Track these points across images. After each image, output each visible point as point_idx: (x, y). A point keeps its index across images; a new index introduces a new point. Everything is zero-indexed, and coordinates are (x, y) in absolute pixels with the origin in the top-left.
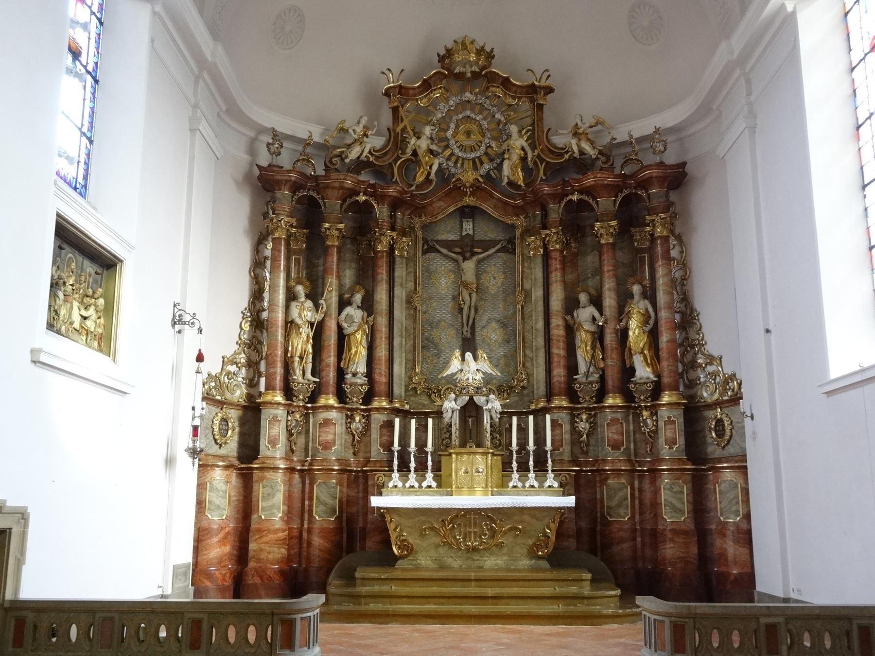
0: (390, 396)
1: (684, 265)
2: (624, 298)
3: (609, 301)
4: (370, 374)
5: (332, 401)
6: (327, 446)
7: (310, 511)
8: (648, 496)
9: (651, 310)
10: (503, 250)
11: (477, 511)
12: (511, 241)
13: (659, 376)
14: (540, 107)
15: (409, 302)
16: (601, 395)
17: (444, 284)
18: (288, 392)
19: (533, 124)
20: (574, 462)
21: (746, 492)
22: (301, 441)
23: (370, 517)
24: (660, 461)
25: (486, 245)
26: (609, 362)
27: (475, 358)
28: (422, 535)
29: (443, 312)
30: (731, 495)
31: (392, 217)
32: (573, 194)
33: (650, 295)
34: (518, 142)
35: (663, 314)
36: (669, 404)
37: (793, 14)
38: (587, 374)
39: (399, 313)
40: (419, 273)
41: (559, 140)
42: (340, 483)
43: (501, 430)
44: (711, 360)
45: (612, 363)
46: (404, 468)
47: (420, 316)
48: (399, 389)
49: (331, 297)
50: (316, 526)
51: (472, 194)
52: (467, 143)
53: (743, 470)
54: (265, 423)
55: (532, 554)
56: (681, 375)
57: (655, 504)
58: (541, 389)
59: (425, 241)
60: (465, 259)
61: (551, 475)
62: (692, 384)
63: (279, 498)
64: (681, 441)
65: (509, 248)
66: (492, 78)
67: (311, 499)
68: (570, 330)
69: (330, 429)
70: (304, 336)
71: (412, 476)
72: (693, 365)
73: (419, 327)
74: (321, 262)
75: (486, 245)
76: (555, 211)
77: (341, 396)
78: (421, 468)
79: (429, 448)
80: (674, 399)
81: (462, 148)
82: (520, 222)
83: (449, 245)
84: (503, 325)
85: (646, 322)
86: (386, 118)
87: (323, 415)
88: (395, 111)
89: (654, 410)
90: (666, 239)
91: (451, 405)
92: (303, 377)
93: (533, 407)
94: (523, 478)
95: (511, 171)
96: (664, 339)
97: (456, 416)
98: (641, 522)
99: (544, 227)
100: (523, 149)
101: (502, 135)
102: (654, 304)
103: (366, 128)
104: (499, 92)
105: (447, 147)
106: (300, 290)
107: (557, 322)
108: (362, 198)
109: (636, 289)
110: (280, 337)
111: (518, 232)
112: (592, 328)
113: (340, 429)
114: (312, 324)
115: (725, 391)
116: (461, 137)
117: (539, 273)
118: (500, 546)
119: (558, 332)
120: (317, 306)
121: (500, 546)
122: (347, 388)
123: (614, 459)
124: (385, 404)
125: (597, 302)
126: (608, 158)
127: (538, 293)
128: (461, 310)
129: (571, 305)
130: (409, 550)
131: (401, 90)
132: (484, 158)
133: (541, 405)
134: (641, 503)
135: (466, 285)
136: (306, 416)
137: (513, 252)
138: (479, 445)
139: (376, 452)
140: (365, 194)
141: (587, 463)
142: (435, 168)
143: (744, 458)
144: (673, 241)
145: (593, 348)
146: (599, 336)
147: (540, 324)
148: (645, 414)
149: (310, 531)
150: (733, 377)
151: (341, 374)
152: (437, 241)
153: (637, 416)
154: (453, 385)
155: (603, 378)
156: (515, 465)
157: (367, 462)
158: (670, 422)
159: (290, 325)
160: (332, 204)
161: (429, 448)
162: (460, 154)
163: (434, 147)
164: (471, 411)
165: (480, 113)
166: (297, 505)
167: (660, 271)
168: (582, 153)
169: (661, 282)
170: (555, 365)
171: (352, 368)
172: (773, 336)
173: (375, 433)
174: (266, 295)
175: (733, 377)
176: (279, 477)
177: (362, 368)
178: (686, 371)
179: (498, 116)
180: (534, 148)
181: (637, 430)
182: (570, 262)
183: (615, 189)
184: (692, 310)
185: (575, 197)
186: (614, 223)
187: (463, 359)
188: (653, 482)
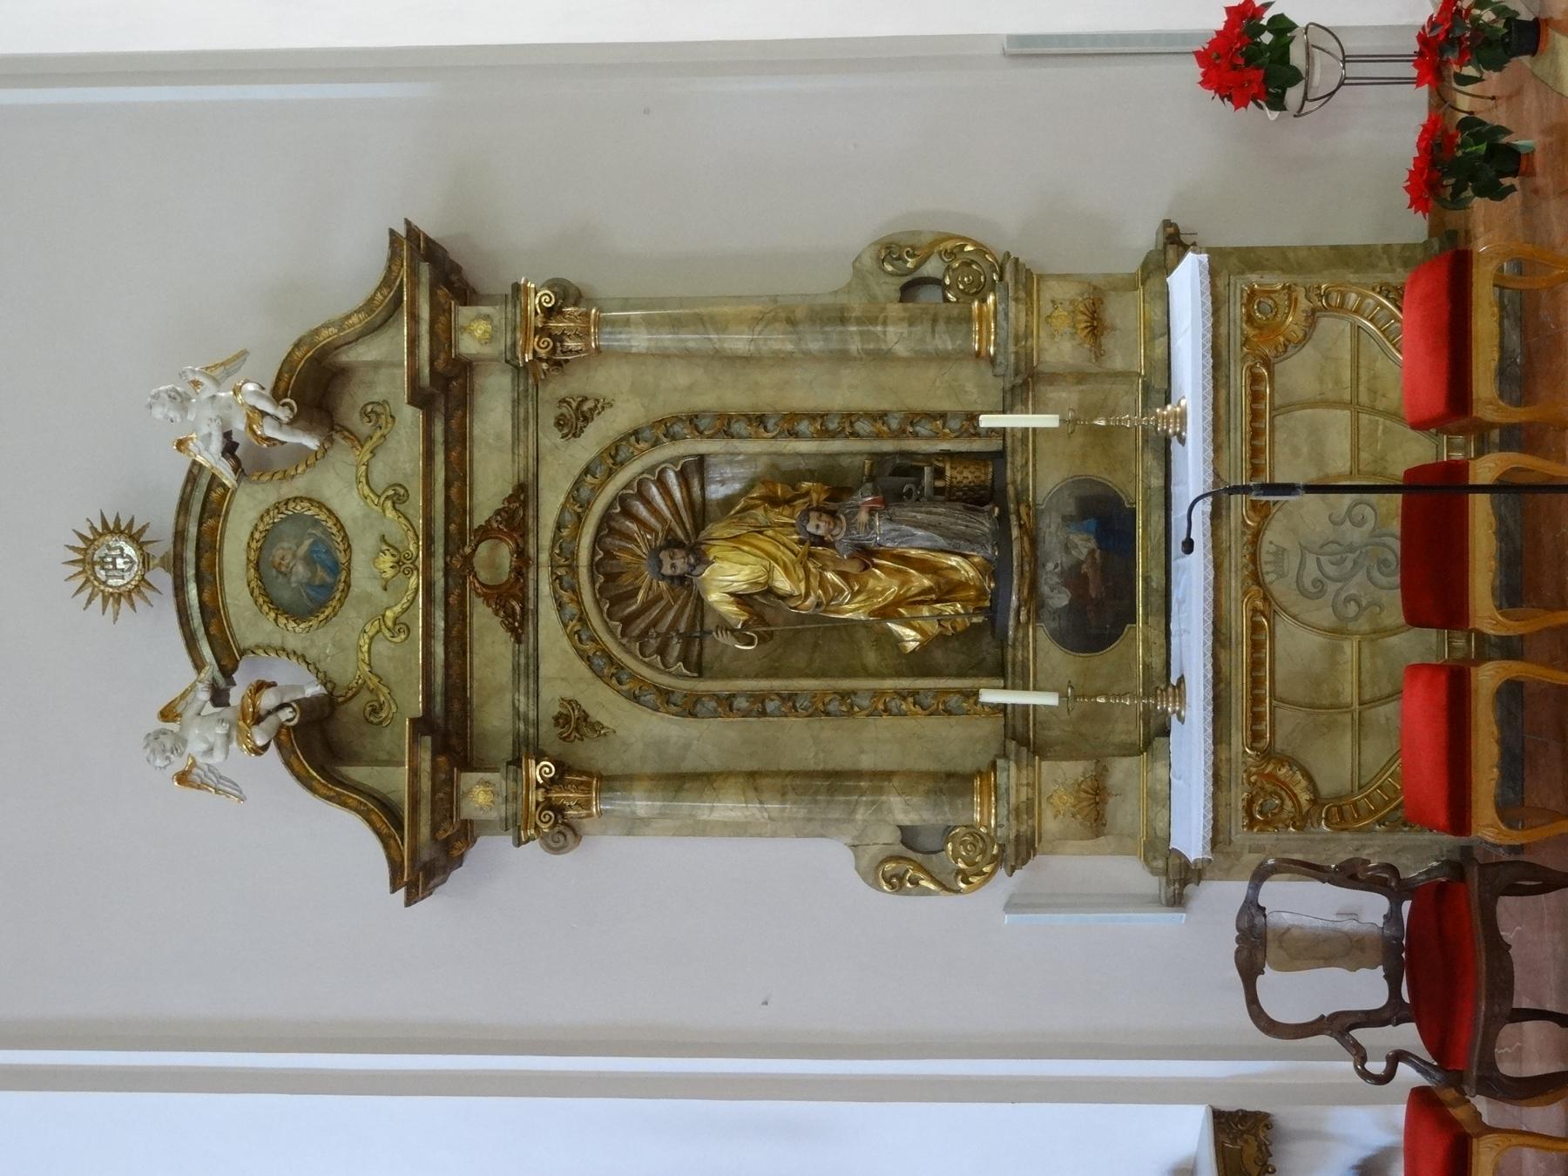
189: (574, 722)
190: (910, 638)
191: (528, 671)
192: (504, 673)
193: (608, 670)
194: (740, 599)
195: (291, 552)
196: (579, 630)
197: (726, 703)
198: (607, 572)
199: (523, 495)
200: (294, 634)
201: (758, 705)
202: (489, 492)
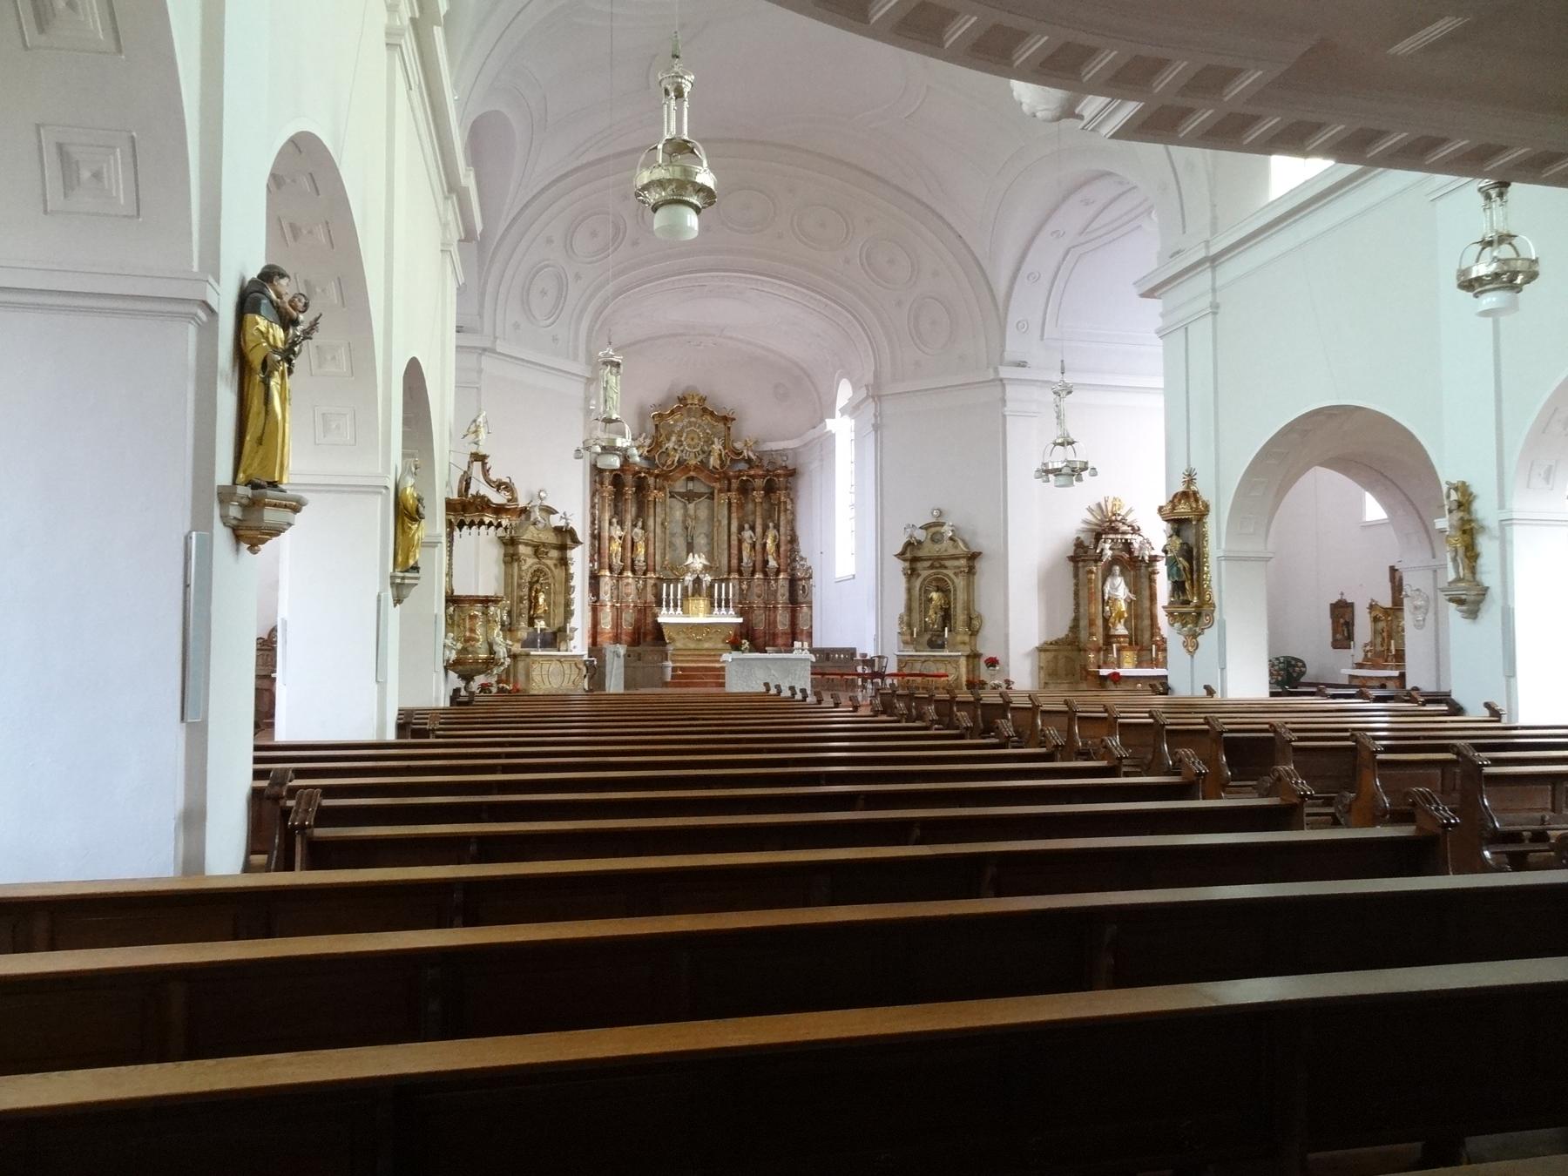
0: (655, 571)
1: (793, 513)
2: (765, 528)
3: (759, 529)
4: (646, 561)
5: (630, 574)
6: (628, 595)
7: (621, 625)
8: (772, 618)
9: (777, 534)
10: (708, 498)
11: (702, 624)
12: (712, 494)
13: (779, 565)
14: (729, 428)
15: (663, 524)
16: (753, 573)
17: (678, 514)
18: (611, 570)
19: (725, 437)
20: (740, 603)
21: (811, 616)
22: (616, 592)
23: (647, 627)
24: (779, 603)
25: (700, 495)
26: (758, 558)
27: (699, 557)
28: (678, 633)
29: (679, 529)
30: (805, 618)
31: (655, 482)
32: (743, 476)
33: (777, 527)
34: (717, 446)
35: (783, 538)
36: (783, 578)
37: (834, 434)
38: (747, 564)
39: (658, 530)
40: (668, 510)
41: (739, 445)
42: (634, 612)
43: (711, 586)
44: (802, 559)
45: (759, 558)
46: (668, 605)
47: (668, 532)
48: (658, 568)
49: (628, 524)
50: (623, 631)
51: (694, 471)
52: (692, 443)
53: (811, 607)
54: (602, 584)
55: (724, 641)
56: (789, 565)
57: (775, 622)
58: (725, 569)
59: (670, 493)
60: (690, 503)
61: (731, 609)
62: (793, 569)
63: (610, 618)
64: (787, 594)
65: (711, 496)
66: (705, 410)
67: (621, 619)
68: (740, 542)
69: (629, 587)
70: (617, 543)
71: (672, 609)
72: (794, 560)
73: (668, 536)
74: (620, 504)
75: (700, 495)
76: (735, 484)
77: (634, 571)
78: (676, 606)
79: (679, 597)
80: (786, 576)
81: (689, 446)
82: (717, 485)
83: (682, 495)
84: (707, 536)
85: (774, 541)
86: (650, 426)
87: (626, 581)
88: (657, 426)
89: (776, 580)
90: (785, 503)
91: (689, 578)
92: (617, 561)
93: (721, 577)
94: (720, 610)
95: (714, 461)
96: (782, 549)
97: (691, 583)
98: (769, 629)
99: (729, 490)
100: (720, 450)
101: (709, 442)
102: (778, 531)
103: (644, 439)
104: (709, 418)
105: (682, 445)
106: (614, 520)
107: (734, 538)
108: (643, 475)
109: (771, 525)
110: (607, 545)
111: (716, 491)
112: (750, 541)
113: (633, 587)
114: (620, 538)
115: (806, 574)
116: (689, 441)
117: (726, 512)
118: (711, 638)
119: (734, 542)
120: (622, 529)
121: (711, 638)
122: (637, 568)
123: (757, 602)
124: (653, 575)
125: (753, 528)
126: (761, 460)
127: (725, 522)
128: (687, 528)
129: (741, 529)
130: (672, 640)
131: (660, 415)
132: (700, 452)
133: (725, 576)
134: (769, 620)
135: (690, 516)
136: (618, 581)
137: (713, 499)
138: (700, 596)
139: (650, 598)
140: (644, 473)
141: (745, 604)
142: (676, 459)
143: (811, 603)
144: (788, 501)
145: (751, 551)
146: (753, 546)
147: (726, 538)
148: (773, 582)
149: (621, 634)
150: (810, 568)
151: (633, 561)
152: (676, 493)
153: (769, 583)
154: (688, 569)
155: (754, 565)
156: (716, 605)
157: (645, 603)
158: (783, 586)
159: (611, 538)
160: (629, 478)
161: (679, 597)
162: (689, 449)
163: (676, 447)
164: (698, 581)
165: (698, 428)
166: (615, 621)
167: (782, 518)
168: (749, 457)
169: (782, 523)
170: (732, 558)
171: (638, 558)
172: (823, 555)
173: (649, 589)
174: (596, 522)
175: (810, 568)
176: (608, 609)
177: (642, 559)
178: (791, 562)
179: (708, 431)
180: (725, 450)
181: (769, 589)
182: (741, 506)
183: (763, 477)
184: (795, 536)
185: (744, 478)
186: (762, 492)
187: (694, 557)
188: (774, 612)
189: (919, 575)
190: (927, 619)
191: (925, 569)
193: (924, 580)
194: (932, 598)
195: (938, 537)
196: (927, 577)
197: (920, 595)
199: (946, 568)
200: (929, 537)
201: (920, 600)
202: (948, 563)
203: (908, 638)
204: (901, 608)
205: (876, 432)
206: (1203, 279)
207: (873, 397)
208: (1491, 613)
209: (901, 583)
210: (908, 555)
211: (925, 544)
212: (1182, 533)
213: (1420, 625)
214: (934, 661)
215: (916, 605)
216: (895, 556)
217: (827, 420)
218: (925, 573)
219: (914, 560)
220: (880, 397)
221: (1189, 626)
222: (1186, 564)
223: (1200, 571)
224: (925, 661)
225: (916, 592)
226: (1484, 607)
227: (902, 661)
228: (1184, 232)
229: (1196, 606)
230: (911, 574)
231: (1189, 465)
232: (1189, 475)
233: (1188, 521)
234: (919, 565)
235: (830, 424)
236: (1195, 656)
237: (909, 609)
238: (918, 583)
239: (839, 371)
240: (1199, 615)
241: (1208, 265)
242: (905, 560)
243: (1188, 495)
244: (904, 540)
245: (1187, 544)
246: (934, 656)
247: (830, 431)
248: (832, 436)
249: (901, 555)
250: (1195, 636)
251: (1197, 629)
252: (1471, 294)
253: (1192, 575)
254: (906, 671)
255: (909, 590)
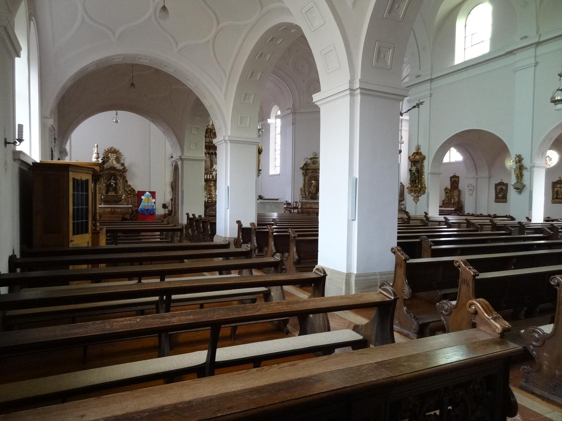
189: (308, 175)
190: (311, 190)
191: (310, 173)
192: (310, 172)
193: (310, 176)
195: (315, 162)
196: (311, 175)
198: (313, 177)
201: (308, 183)
203: (304, 196)
204: (301, 186)
205: (293, 125)
206: (427, 86)
207: (293, 113)
208: (526, 192)
209: (302, 177)
210: (305, 168)
211: (310, 164)
212: (416, 166)
213: (471, 195)
214: (314, 204)
215: (306, 185)
216: (300, 168)
217: (268, 120)
218: (310, 174)
219: (307, 170)
220: (295, 113)
221: (417, 194)
222: (417, 174)
223: (421, 177)
224: (311, 204)
225: (307, 181)
226: (523, 190)
227: (302, 203)
228: (420, 69)
229: (420, 188)
230: (305, 175)
231: (418, 144)
232: (418, 147)
233: (418, 161)
234: (308, 171)
235: (269, 121)
236: (417, 203)
237: (304, 186)
238: (307, 178)
239: (273, 102)
240: (420, 190)
241: (430, 81)
242: (303, 170)
243: (418, 153)
244: (304, 163)
245: (417, 168)
246: (314, 202)
247: (269, 123)
248: (269, 125)
249: (302, 168)
250: (418, 197)
251: (419, 195)
252: (553, 104)
253: (419, 178)
254: (304, 207)
255: (305, 180)
